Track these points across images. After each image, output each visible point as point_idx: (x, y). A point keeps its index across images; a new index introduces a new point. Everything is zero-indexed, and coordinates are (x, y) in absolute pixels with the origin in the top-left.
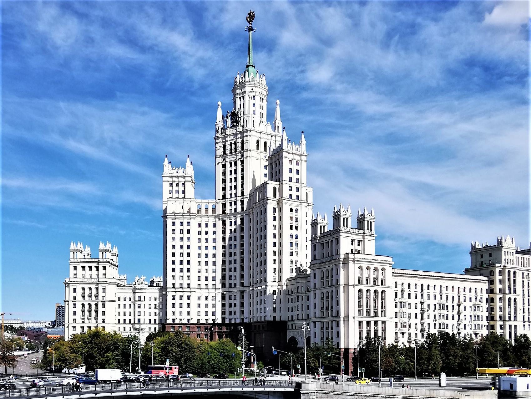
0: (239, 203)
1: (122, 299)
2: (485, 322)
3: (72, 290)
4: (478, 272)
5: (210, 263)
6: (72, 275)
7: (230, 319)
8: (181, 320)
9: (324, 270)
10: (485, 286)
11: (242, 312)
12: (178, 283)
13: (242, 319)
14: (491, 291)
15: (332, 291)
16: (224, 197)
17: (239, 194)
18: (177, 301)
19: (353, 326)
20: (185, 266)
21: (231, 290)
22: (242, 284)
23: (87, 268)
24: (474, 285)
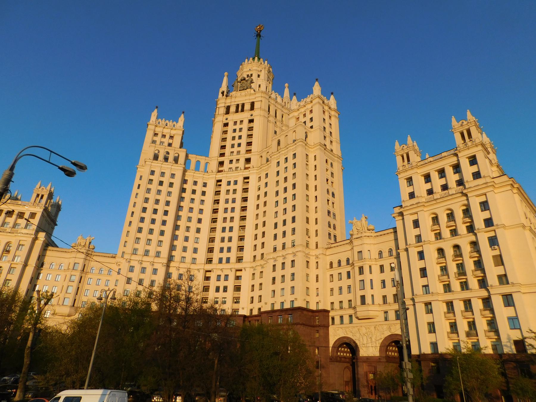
11: (237, 301)
21: (220, 266)
22: (240, 259)
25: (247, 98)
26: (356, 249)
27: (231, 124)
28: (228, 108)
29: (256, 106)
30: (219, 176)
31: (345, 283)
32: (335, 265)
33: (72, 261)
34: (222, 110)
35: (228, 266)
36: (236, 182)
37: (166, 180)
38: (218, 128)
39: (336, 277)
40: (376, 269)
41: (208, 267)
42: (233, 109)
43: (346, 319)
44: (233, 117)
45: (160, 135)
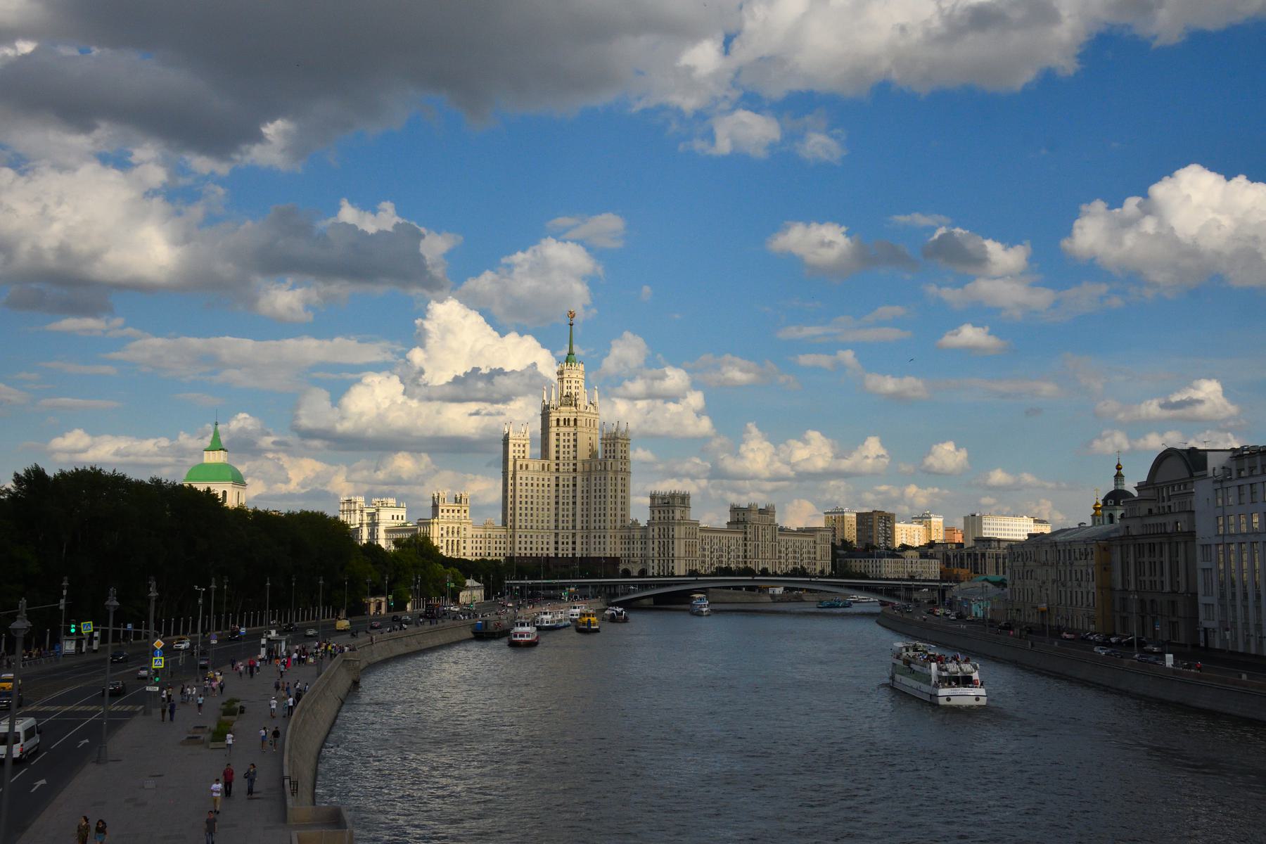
0: (571, 465)
1: (474, 536)
2: (740, 560)
3: (440, 529)
4: (735, 526)
5: (546, 510)
6: (440, 517)
7: (563, 554)
8: (525, 554)
9: (661, 527)
10: (741, 536)
11: (574, 549)
12: (523, 524)
13: (574, 554)
14: (746, 539)
15: (668, 541)
16: (558, 458)
17: (571, 458)
18: (523, 539)
19: (683, 563)
20: (529, 512)
21: (564, 531)
22: (574, 527)
23: (451, 511)
24: (735, 536)
25: (572, 414)
26: (632, 533)
27: (561, 434)
28: (558, 420)
29: (578, 423)
30: (557, 475)
31: (627, 546)
32: (623, 537)
33: (488, 533)
34: (554, 423)
35: (567, 531)
36: (568, 480)
37: (530, 482)
38: (553, 437)
39: (623, 543)
40: (639, 542)
41: (557, 531)
42: (562, 423)
43: (627, 561)
44: (563, 430)
45: (517, 445)
